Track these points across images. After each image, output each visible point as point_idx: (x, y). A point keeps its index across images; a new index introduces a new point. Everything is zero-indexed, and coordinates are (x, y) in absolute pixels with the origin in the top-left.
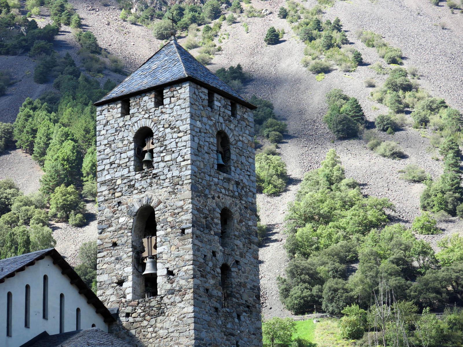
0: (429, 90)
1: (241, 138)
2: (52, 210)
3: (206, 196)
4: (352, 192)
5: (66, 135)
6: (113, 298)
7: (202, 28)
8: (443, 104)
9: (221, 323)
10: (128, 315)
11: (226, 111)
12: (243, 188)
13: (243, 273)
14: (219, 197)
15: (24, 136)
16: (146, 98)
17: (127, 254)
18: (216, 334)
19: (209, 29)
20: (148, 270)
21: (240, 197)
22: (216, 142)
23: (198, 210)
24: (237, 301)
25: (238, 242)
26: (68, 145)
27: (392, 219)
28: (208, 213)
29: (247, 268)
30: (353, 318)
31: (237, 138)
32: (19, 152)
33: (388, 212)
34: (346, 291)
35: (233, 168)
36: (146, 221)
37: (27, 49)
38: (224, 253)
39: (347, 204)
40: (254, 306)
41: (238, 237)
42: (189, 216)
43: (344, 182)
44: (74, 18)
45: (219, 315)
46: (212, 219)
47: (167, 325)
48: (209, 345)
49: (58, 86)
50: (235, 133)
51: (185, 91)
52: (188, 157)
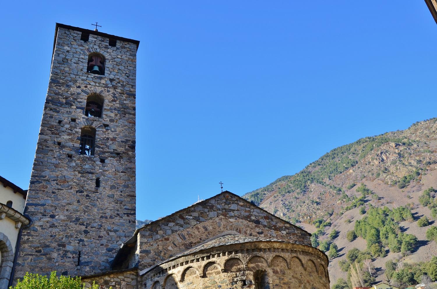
1: (119, 57)
3: (68, 86)
7: (415, 180)
9: (74, 164)
12: (119, 83)
13: (112, 131)
14: (86, 87)
18: (65, 173)
19: (417, 180)
21: (115, 88)
22: (87, 57)
24: (102, 150)
25: (109, 113)
26: (373, 231)
28: (70, 96)
29: (118, 129)
31: (114, 57)
35: (106, 72)
37: (356, 206)
38: (87, 120)
40: (123, 152)
41: (111, 110)
45: (73, 160)
46: (76, 99)
48: (54, 180)
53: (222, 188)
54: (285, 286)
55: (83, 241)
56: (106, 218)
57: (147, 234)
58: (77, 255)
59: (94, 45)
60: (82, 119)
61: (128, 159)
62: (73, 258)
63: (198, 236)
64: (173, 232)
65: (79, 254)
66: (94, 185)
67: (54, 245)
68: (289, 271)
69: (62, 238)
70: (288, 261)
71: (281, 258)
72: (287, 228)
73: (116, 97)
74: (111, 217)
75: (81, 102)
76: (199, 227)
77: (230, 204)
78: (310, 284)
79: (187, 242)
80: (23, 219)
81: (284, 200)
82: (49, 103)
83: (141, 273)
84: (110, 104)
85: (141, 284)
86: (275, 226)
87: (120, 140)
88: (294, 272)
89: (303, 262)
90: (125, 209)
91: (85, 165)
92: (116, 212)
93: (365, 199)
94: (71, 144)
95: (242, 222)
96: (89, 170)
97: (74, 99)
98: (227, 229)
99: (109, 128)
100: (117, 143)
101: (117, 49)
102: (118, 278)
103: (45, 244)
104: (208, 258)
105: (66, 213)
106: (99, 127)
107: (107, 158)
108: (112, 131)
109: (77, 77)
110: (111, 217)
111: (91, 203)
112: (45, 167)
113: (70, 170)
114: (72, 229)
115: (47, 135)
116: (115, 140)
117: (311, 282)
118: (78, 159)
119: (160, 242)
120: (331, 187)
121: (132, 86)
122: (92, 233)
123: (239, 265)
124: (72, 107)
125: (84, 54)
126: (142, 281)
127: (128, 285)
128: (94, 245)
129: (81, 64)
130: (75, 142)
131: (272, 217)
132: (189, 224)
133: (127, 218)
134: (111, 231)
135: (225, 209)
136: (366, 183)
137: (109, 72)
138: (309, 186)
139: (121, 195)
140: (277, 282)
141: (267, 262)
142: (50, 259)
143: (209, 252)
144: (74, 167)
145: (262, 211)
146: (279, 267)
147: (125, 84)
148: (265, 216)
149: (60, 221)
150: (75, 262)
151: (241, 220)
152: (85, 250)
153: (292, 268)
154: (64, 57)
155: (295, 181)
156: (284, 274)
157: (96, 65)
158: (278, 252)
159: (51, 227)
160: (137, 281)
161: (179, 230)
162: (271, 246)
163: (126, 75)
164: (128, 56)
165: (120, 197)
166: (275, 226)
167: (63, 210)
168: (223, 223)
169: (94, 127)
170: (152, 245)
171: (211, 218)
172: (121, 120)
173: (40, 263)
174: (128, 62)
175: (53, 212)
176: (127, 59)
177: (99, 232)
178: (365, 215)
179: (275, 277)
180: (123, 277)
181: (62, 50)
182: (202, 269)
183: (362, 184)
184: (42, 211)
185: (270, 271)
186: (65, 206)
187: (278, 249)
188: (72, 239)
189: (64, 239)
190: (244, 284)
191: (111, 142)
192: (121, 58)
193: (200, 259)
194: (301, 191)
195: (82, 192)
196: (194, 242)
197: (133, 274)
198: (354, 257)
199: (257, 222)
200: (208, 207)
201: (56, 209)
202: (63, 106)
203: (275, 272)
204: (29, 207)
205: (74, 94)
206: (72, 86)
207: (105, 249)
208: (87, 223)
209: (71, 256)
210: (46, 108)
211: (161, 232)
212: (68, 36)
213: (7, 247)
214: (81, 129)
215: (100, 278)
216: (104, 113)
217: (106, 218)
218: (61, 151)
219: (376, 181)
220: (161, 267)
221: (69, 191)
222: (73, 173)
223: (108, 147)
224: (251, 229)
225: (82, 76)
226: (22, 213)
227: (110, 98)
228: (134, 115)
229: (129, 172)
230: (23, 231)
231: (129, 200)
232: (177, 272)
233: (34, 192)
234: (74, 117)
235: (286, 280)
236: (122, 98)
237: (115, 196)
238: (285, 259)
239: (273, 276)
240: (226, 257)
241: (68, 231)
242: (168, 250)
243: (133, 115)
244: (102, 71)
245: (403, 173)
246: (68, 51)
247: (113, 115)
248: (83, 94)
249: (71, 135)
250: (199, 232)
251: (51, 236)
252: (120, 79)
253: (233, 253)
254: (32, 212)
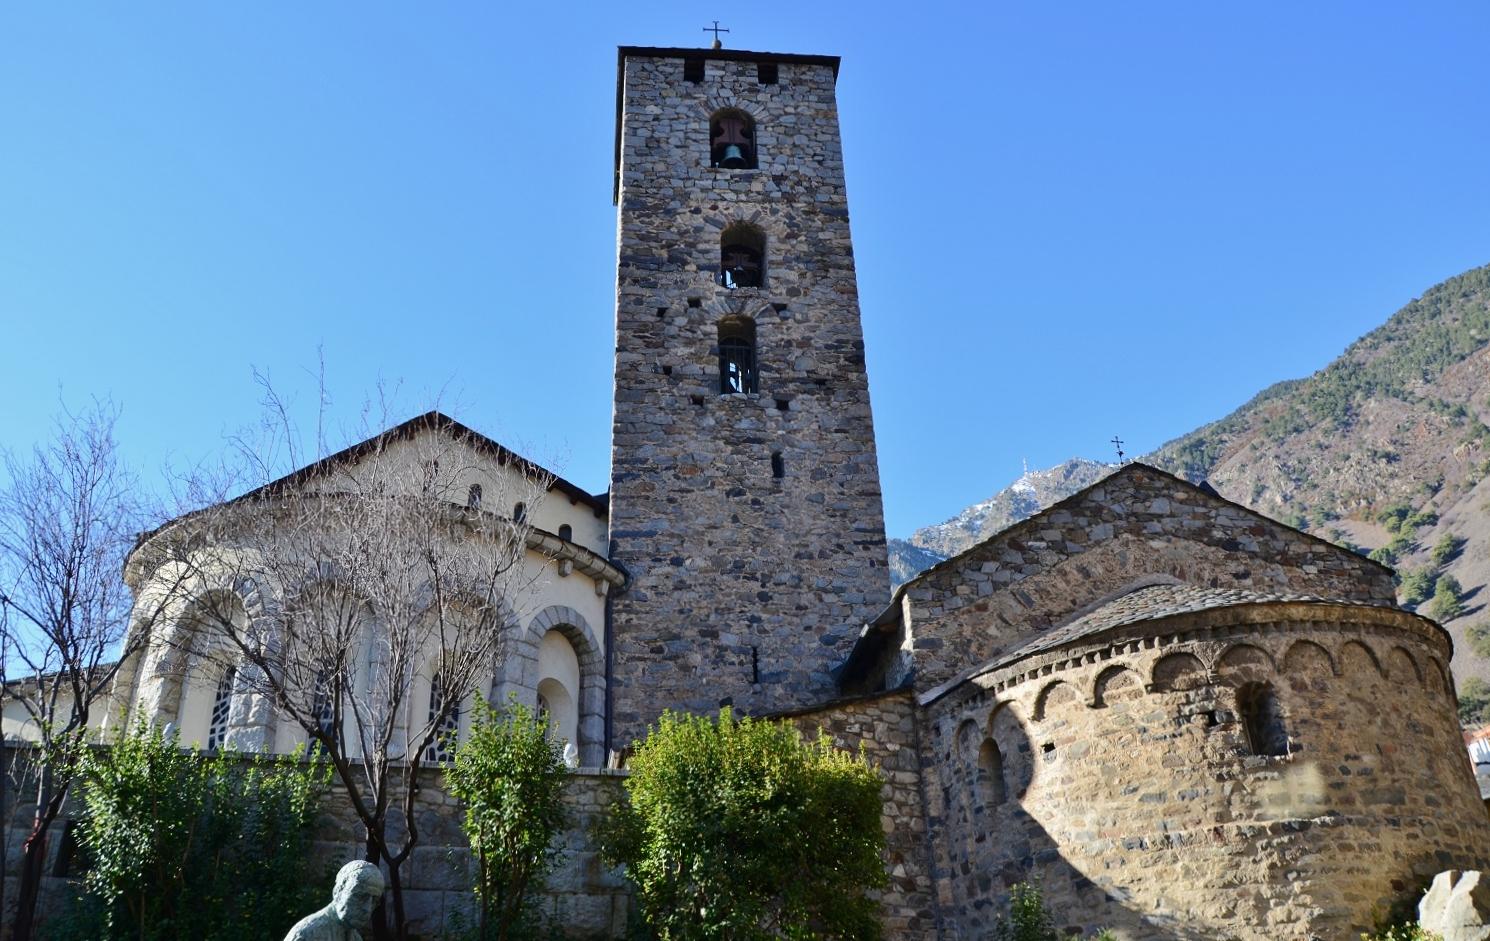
1: (790, 110)
3: (668, 212)
9: (712, 422)
11: (741, 79)
12: (799, 183)
13: (799, 322)
14: (714, 208)
18: (693, 447)
21: (789, 199)
22: (707, 126)
23: (642, 238)
25: (783, 272)
28: (677, 237)
31: (776, 113)
35: (761, 158)
40: (834, 376)
41: (786, 263)
45: (707, 409)
46: (692, 245)
48: (667, 469)
50: (770, 105)
53: (1121, 454)
54: (1329, 723)
55: (758, 620)
56: (811, 557)
57: (928, 595)
58: (750, 658)
59: (721, 88)
60: (717, 295)
61: (850, 394)
62: (741, 663)
63: (1066, 595)
64: (996, 586)
65: (755, 655)
66: (768, 473)
67: (691, 633)
68: (1337, 683)
69: (708, 616)
70: (1334, 654)
71: (1313, 648)
72: (1317, 557)
73: (797, 226)
74: (822, 555)
75: (707, 252)
76: (1068, 569)
77: (1147, 498)
78: (1400, 716)
79: (1038, 613)
80: (611, 572)
81: (1282, 456)
82: (628, 266)
83: (924, 699)
84: (783, 247)
85: (926, 728)
86: (1283, 553)
87: (820, 343)
88: (1353, 683)
89: (1379, 654)
90: (858, 530)
91: (740, 420)
92: (834, 541)
94: (696, 368)
95: (1186, 548)
96: (751, 434)
97: (688, 245)
98: (1145, 571)
99: (788, 314)
100: (814, 352)
101: (783, 88)
102: (865, 714)
103: (670, 632)
104: (1106, 654)
105: (708, 551)
106: (763, 314)
107: (792, 397)
108: (799, 322)
109: (689, 183)
110: (822, 555)
111: (767, 522)
112: (641, 436)
113: (704, 438)
114: (727, 590)
115: (634, 350)
116: (810, 345)
117: (1403, 710)
118: (721, 408)
119: (965, 616)
120: (1431, 405)
121: (836, 187)
122: (781, 600)
123: (1193, 670)
124: (687, 268)
125: (699, 119)
126: (927, 720)
127: (892, 730)
128: (786, 630)
129: (693, 147)
130: (707, 363)
131: (1274, 528)
132: (1037, 562)
133: (865, 554)
134: (826, 591)
135: (1134, 514)
137: (769, 159)
138: (1360, 406)
139: (842, 494)
140: (1305, 712)
141: (1272, 660)
142: (686, 669)
143: (1107, 640)
144: (712, 429)
145: (1242, 514)
146: (1309, 672)
147: (814, 184)
148: (1253, 525)
149: (695, 573)
150: (746, 675)
151: (1184, 543)
152: (767, 642)
153: (1347, 674)
154: (649, 134)
155: (1314, 395)
156: (1323, 689)
157: (733, 143)
158: (1304, 630)
159: (676, 588)
160: (915, 721)
161: (1013, 580)
162: (1282, 615)
163: (816, 158)
164: (814, 105)
165: (840, 500)
166: (1283, 553)
167: (700, 543)
168: (1133, 553)
169: (749, 314)
170: (944, 625)
171: (1098, 543)
172: (817, 288)
173: (664, 678)
174: (817, 121)
175: (676, 551)
176: (812, 112)
177: (795, 595)
179: (1298, 701)
180: (877, 712)
181: (641, 118)
182: (1090, 685)
184: (651, 550)
185: (1282, 684)
186: (703, 534)
187: (1302, 621)
188: (731, 616)
189: (713, 617)
190: (1212, 722)
191: (798, 352)
192: (795, 114)
193: (1084, 660)
194: (1336, 423)
195: (740, 493)
196: (1057, 610)
197: (901, 703)
199: (1231, 545)
200: (1088, 513)
201: (683, 542)
202: (664, 269)
203: (1298, 687)
204: (618, 540)
205: (687, 232)
206: (680, 211)
207: (817, 638)
208: (762, 575)
209: (734, 659)
210: (622, 279)
211: (963, 590)
212: (652, 76)
213: (587, 642)
214: (717, 323)
215: (821, 714)
216: (770, 272)
217: (811, 557)
218: (675, 390)
220: (975, 684)
221: (709, 493)
222: (711, 445)
223: (791, 365)
224: (1215, 565)
225: (701, 179)
226: (605, 556)
227: (782, 228)
228: (851, 268)
229: (854, 429)
230: (616, 602)
231: (863, 504)
232: (1021, 697)
233: (625, 503)
234: (694, 296)
235: (1330, 707)
236: (814, 225)
237: (827, 497)
238: (1323, 650)
239: (1291, 698)
240: (1156, 652)
241: (721, 597)
242: (987, 637)
243: (848, 269)
244: (749, 160)
246: (656, 118)
247: (793, 276)
248: (710, 228)
249: (694, 343)
250: (1068, 582)
251: (681, 612)
252: (801, 172)
253: (1176, 640)
254: (628, 553)
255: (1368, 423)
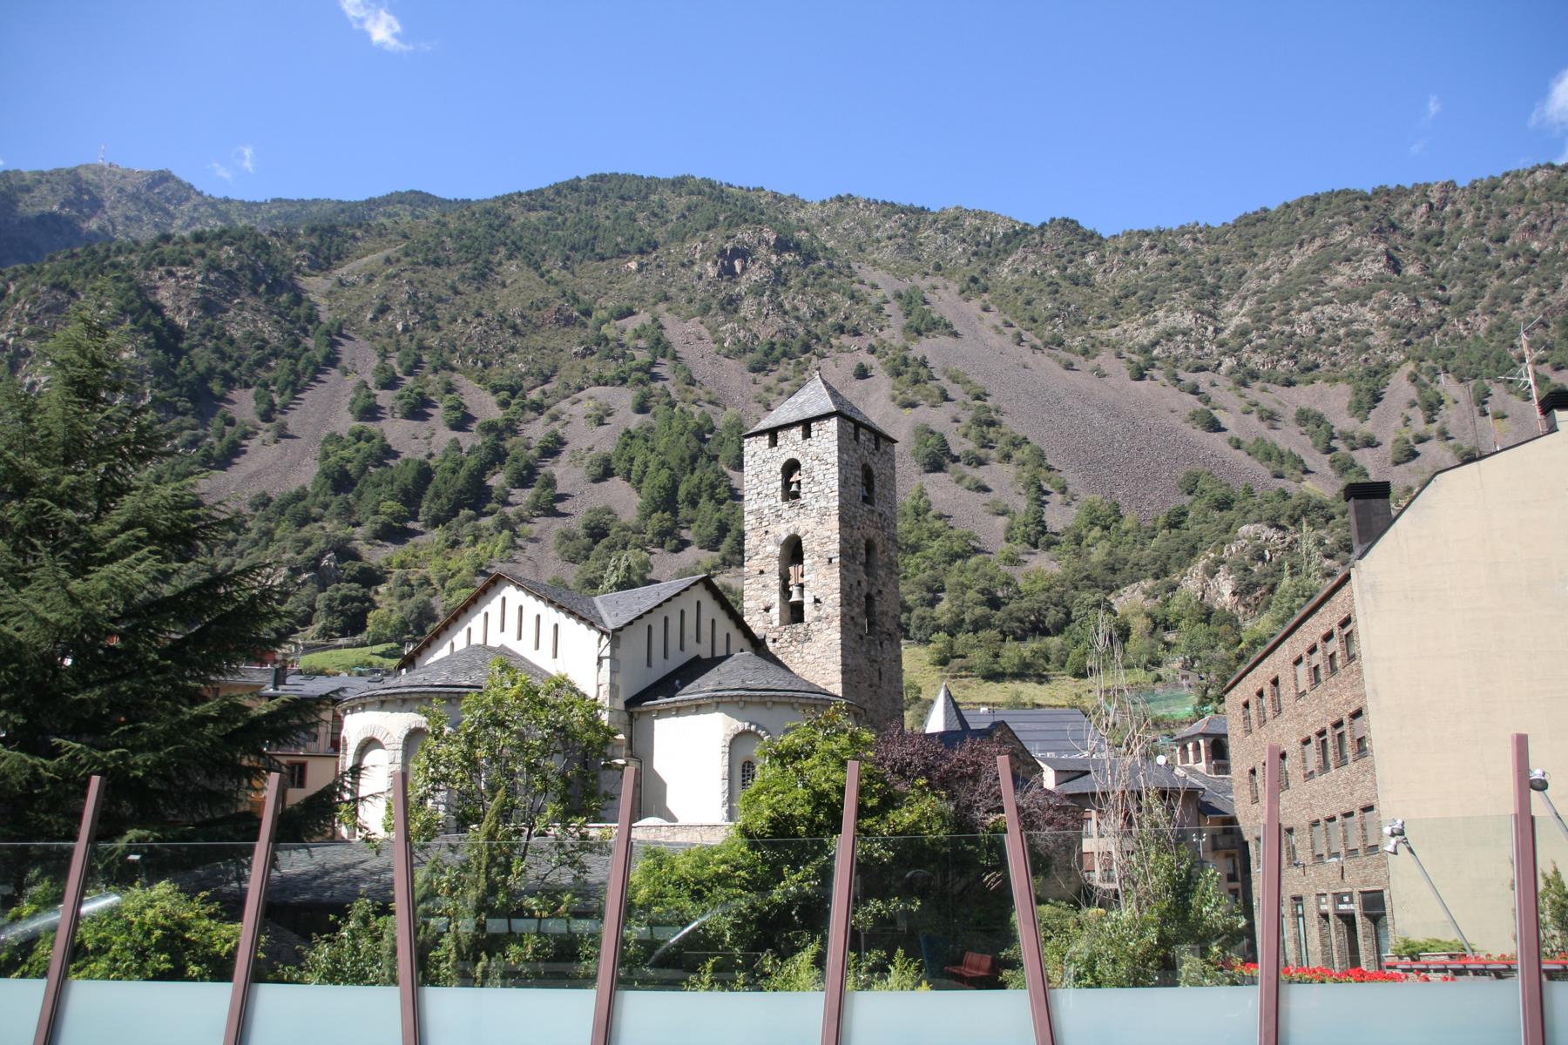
0: (1012, 425)
2: (649, 536)
4: (939, 524)
5: (663, 463)
6: (760, 624)
8: (1025, 441)
10: (774, 641)
15: (622, 465)
16: (794, 431)
17: (774, 581)
19: (799, 363)
20: (795, 598)
21: (883, 529)
26: (665, 473)
27: (976, 551)
30: (941, 645)
32: (617, 479)
33: (973, 543)
34: (933, 619)
36: (793, 551)
37: (624, 381)
39: (935, 535)
42: (837, 546)
43: (931, 514)
44: (670, 351)
47: (813, 651)
49: (654, 416)
51: (833, 424)
52: (836, 488)
93: (655, 370)
136: (667, 319)
138: (500, 264)
155: (462, 232)
178: (646, 418)
183: (655, 320)
198: (597, 532)
219: (693, 326)
245: (768, 329)
255: (504, 285)
